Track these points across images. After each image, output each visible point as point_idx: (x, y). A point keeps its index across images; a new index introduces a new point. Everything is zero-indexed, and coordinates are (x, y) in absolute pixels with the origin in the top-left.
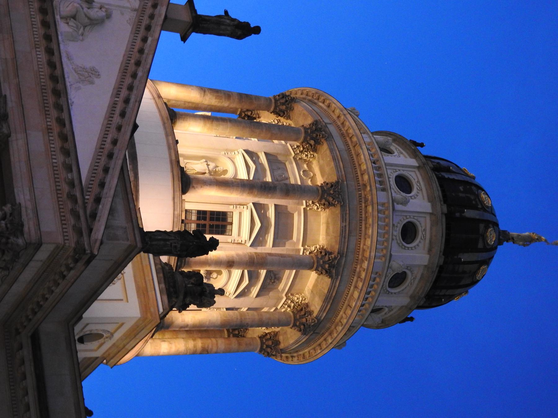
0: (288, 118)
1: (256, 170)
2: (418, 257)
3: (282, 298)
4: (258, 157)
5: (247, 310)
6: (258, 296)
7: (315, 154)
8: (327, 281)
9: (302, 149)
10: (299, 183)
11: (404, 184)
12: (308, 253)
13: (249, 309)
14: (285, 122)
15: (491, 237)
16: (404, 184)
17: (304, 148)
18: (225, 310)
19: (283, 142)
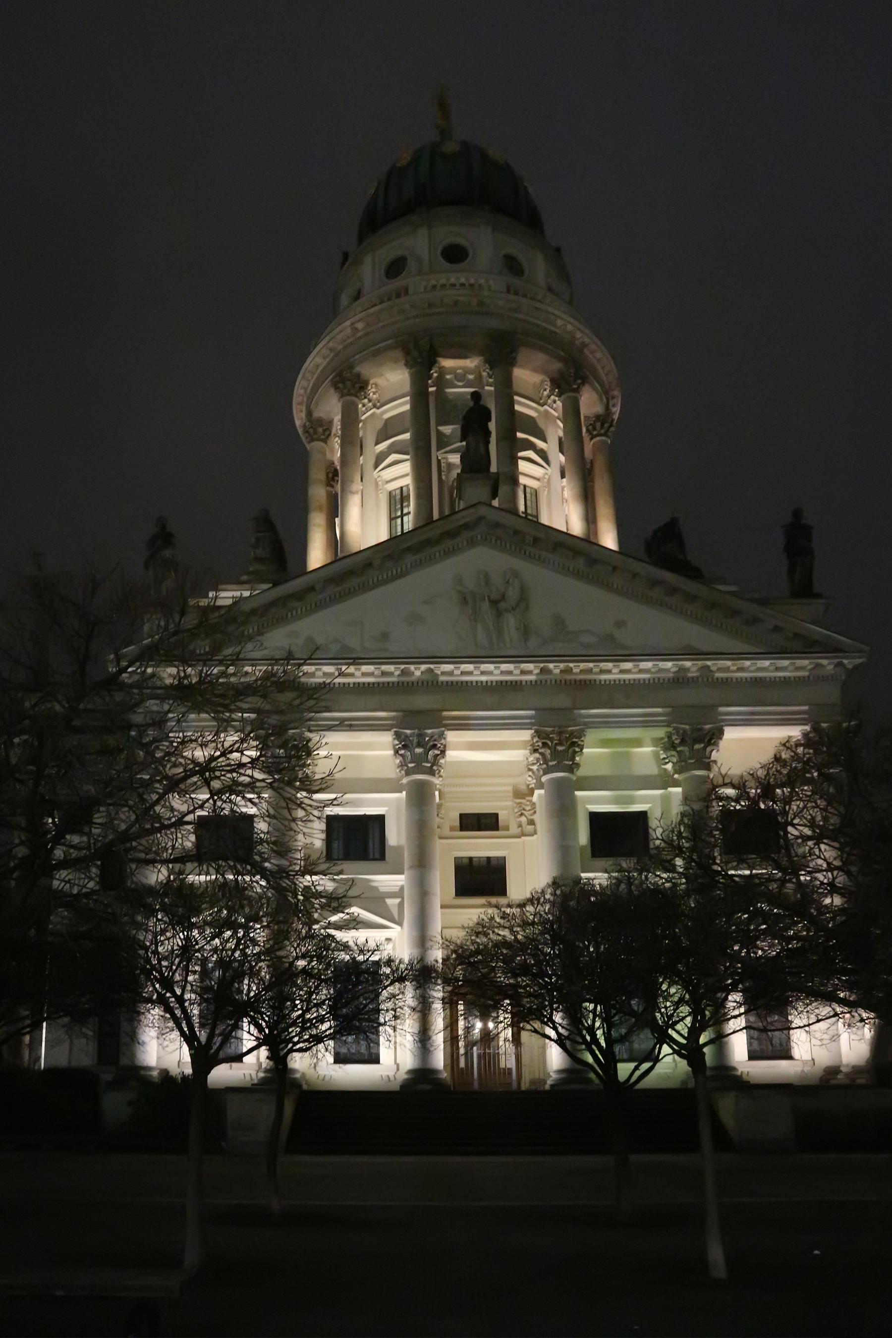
0: (331, 422)
1: (395, 453)
2: (484, 241)
3: (546, 411)
4: (381, 453)
5: (563, 454)
6: (545, 441)
7: (371, 382)
8: (523, 354)
9: (366, 401)
10: (408, 398)
11: (396, 268)
12: (491, 380)
13: (561, 450)
14: (337, 426)
15: (450, 147)
16: (396, 268)
17: (365, 398)
18: (564, 480)
19: (360, 425)
